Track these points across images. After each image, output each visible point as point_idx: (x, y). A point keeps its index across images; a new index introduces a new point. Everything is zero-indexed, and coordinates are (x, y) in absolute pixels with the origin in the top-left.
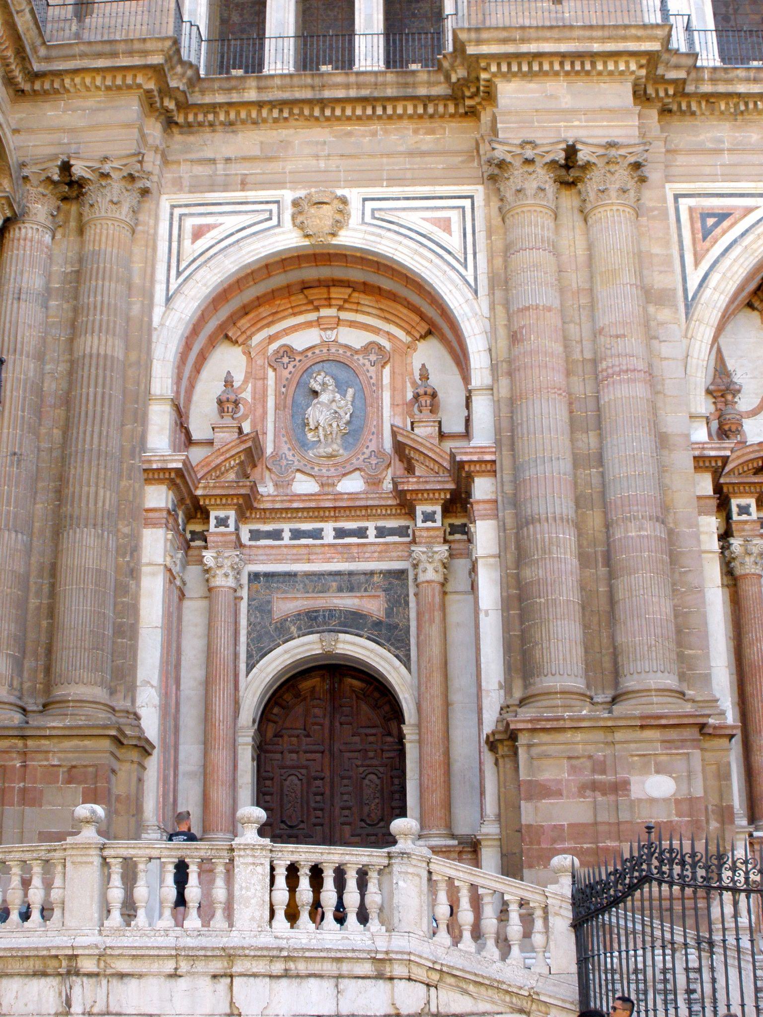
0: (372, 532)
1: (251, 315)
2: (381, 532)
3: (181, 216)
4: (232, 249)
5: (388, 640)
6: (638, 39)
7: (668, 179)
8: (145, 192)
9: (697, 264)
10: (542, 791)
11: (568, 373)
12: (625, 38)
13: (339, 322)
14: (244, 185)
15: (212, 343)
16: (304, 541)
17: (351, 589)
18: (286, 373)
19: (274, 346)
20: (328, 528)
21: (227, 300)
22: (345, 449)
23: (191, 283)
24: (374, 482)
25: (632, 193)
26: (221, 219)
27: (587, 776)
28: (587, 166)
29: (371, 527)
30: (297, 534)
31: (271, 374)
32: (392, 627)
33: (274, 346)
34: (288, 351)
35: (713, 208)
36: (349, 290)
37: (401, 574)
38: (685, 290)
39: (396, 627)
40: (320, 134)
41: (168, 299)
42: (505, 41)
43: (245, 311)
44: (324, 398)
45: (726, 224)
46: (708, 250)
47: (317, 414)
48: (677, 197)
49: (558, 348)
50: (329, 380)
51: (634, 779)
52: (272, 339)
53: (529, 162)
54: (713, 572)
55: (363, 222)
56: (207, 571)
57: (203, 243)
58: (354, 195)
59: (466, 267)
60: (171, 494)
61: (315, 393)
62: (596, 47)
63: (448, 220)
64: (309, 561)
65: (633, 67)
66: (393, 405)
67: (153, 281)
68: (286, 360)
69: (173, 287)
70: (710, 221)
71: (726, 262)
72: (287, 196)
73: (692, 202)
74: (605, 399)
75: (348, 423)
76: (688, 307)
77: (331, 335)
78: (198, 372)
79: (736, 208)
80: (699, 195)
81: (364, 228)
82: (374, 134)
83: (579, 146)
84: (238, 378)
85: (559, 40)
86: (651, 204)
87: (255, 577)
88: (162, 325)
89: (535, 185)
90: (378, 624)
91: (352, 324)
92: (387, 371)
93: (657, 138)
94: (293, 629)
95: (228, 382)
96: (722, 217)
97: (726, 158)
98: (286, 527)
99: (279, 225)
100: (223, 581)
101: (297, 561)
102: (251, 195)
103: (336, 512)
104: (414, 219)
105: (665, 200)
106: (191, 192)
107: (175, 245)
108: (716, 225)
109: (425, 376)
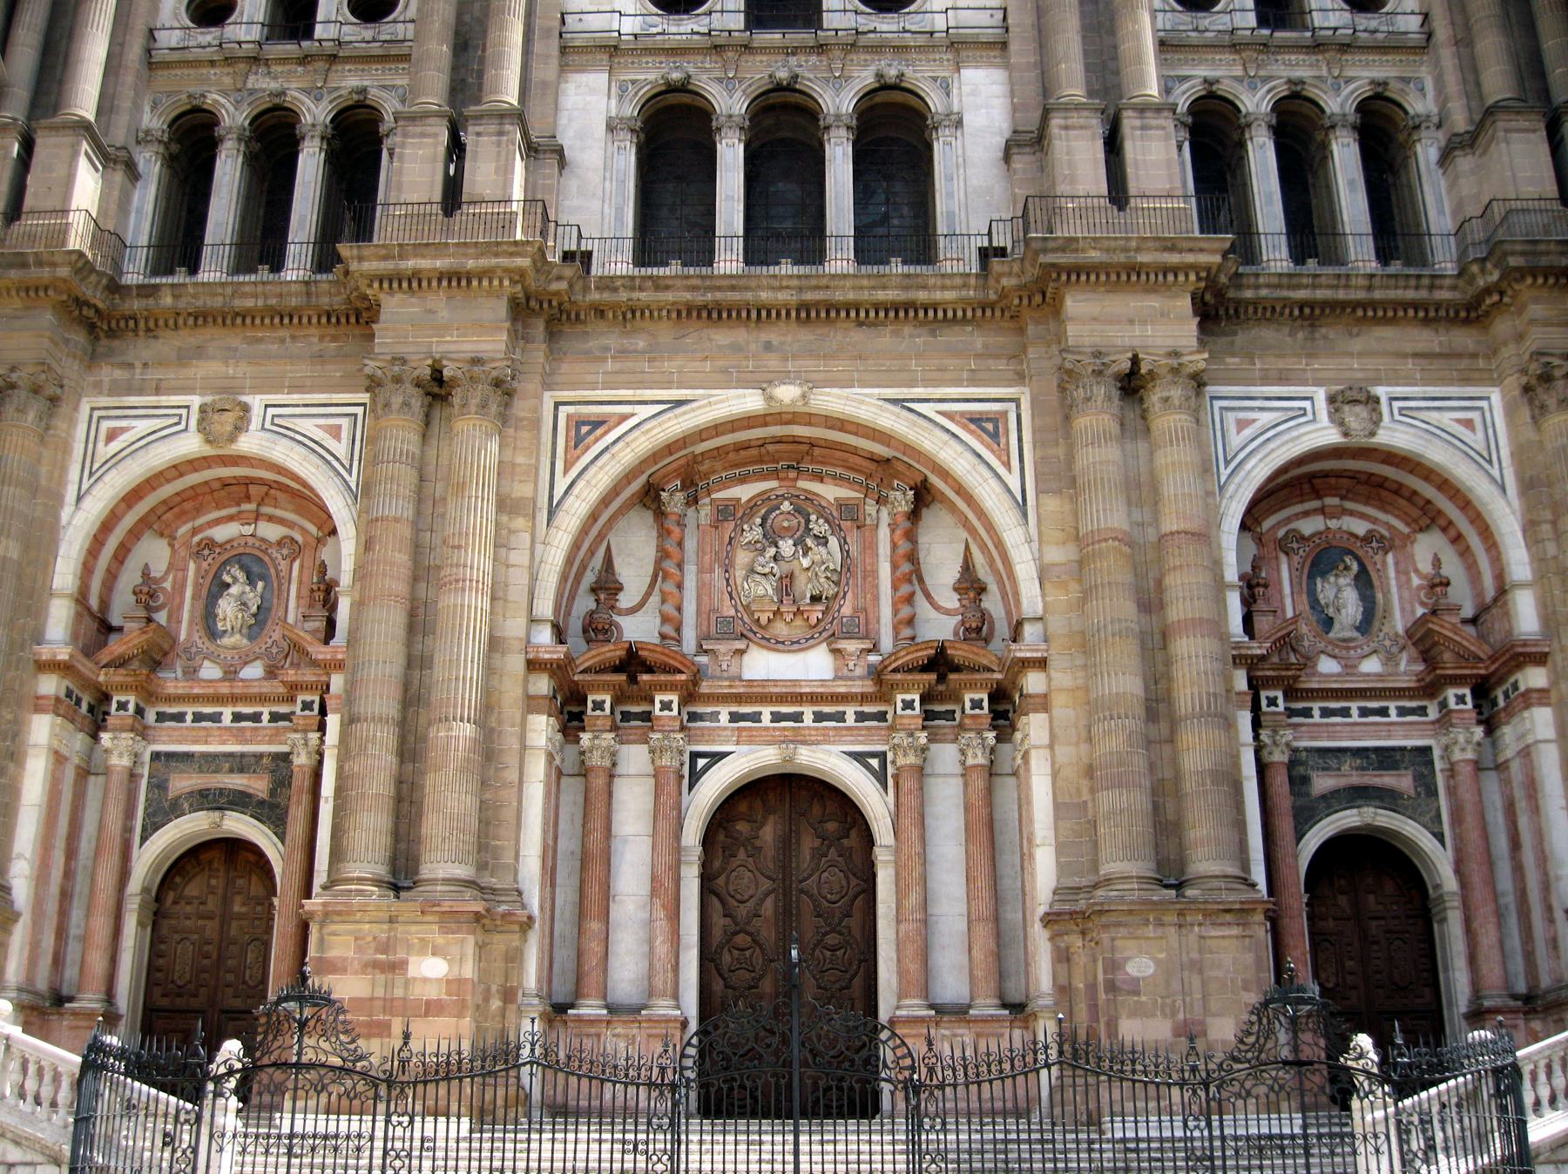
0: (266, 717)
1: (176, 510)
2: (275, 717)
3: (100, 418)
4: (141, 453)
5: (269, 818)
6: (512, 254)
7: (548, 386)
8: (54, 401)
9: (566, 471)
10: (327, 966)
11: (415, 579)
12: (497, 255)
13: (258, 516)
14: (158, 391)
15: (135, 534)
16: (204, 724)
17: (241, 771)
18: (205, 564)
19: (196, 539)
20: (227, 713)
21: (141, 498)
22: (251, 638)
23: (100, 485)
24: (271, 673)
25: (493, 408)
26: (134, 423)
27: (370, 955)
28: (453, 379)
29: (266, 712)
30: (198, 717)
31: (192, 566)
32: (273, 806)
33: (196, 539)
34: (210, 544)
35: (589, 415)
36: (265, 488)
37: (285, 758)
38: (551, 497)
39: (277, 806)
40: (233, 339)
41: (79, 499)
42: (385, 258)
43: (168, 505)
44: (234, 590)
45: (599, 432)
46: (578, 458)
47: (227, 608)
48: (557, 405)
49: (402, 558)
50: (241, 576)
51: (413, 960)
52: (195, 531)
53: (397, 380)
54: (537, 769)
55: (263, 428)
56: (106, 751)
57: (115, 446)
58: (256, 402)
59: (350, 473)
60: (66, 683)
61: (228, 586)
62: (471, 264)
63: (339, 427)
64: (206, 743)
65: (506, 283)
66: (299, 597)
67: (62, 482)
68: (206, 552)
69: (85, 487)
70: (585, 429)
71: (593, 470)
72: (195, 401)
73: (571, 409)
74: (440, 605)
75: (254, 615)
76: (551, 514)
77: (248, 530)
78: (122, 563)
79: (611, 415)
80: (579, 403)
81: (262, 434)
82: (283, 341)
83: (445, 362)
84: (158, 569)
85: (435, 257)
86: (522, 414)
87: (156, 756)
88: (69, 523)
89: (400, 400)
90: (262, 803)
91: (271, 519)
92: (296, 565)
93: (538, 350)
94: (186, 806)
95: (146, 573)
96: (597, 424)
97: (609, 365)
98: (189, 710)
99: (186, 430)
100: (119, 761)
101: (195, 742)
102: (164, 400)
103: (234, 699)
104: (309, 427)
105: (537, 410)
106: (109, 395)
107: (91, 446)
108: (589, 433)
109: (323, 568)
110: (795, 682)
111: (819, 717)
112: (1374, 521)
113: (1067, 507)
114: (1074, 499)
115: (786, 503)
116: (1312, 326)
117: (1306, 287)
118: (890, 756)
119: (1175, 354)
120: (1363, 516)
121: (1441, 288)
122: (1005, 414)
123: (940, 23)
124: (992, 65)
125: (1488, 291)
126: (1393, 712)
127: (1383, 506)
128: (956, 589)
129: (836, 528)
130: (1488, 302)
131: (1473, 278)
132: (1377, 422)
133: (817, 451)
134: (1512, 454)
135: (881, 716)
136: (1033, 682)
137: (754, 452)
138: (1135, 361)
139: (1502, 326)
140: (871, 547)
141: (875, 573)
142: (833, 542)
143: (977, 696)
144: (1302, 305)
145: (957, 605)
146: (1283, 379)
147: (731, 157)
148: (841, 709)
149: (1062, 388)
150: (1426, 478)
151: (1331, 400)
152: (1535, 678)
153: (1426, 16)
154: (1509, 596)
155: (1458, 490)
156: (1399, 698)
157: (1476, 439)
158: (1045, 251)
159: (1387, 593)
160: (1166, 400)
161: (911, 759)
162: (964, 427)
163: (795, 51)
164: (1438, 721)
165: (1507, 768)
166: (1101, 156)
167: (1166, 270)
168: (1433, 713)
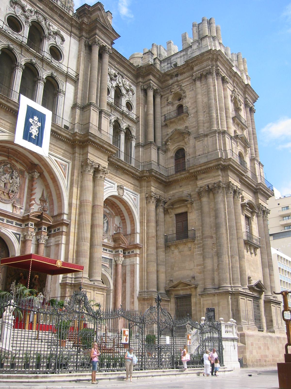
110: (7, 212)
111: (8, 221)
112: (110, 211)
113: (79, 192)
114: (81, 191)
115: (9, 165)
116: (117, 170)
117: (120, 162)
118: (21, 236)
119: (105, 168)
120: (108, 209)
121: (138, 172)
122: (66, 165)
123: (65, 69)
124: (72, 85)
125: (145, 176)
126: (108, 250)
127: (112, 209)
128: (40, 200)
129: (19, 176)
130: (144, 178)
131: (144, 173)
132: (123, 194)
133: (19, 155)
134: (140, 208)
135: (21, 225)
136: (64, 229)
137: (5, 149)
138: (99, 166)
139: (144, 184)
140: (25, 183)
141: (24, 189)
142: (18, 178)
143: (45, 227)
144: (118, 165)
145: (39, 203)
146: (111, 179)
147: (19, 74)
148: (13, 221)
149: (82, 166)
150: (125, 207)
151: (118, 186)
152: (138, 251)
153: (138, 117)
154: (135, 235)
155: (130, 211)
156: (109, 248)
157: (136, 202)
158: (90, 136)
159: (110, 226)
160: (101, 177)
161: (31, 239)
162: (59, 165)
163: (37, 57)
164: (115, 254)
165: (126, 267)
166: (98, 119)
167: (107, 150)
168: (114, 253)
